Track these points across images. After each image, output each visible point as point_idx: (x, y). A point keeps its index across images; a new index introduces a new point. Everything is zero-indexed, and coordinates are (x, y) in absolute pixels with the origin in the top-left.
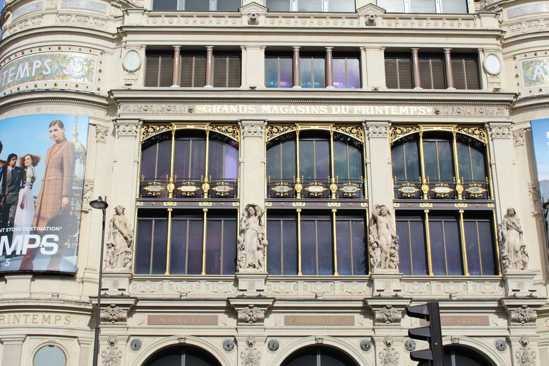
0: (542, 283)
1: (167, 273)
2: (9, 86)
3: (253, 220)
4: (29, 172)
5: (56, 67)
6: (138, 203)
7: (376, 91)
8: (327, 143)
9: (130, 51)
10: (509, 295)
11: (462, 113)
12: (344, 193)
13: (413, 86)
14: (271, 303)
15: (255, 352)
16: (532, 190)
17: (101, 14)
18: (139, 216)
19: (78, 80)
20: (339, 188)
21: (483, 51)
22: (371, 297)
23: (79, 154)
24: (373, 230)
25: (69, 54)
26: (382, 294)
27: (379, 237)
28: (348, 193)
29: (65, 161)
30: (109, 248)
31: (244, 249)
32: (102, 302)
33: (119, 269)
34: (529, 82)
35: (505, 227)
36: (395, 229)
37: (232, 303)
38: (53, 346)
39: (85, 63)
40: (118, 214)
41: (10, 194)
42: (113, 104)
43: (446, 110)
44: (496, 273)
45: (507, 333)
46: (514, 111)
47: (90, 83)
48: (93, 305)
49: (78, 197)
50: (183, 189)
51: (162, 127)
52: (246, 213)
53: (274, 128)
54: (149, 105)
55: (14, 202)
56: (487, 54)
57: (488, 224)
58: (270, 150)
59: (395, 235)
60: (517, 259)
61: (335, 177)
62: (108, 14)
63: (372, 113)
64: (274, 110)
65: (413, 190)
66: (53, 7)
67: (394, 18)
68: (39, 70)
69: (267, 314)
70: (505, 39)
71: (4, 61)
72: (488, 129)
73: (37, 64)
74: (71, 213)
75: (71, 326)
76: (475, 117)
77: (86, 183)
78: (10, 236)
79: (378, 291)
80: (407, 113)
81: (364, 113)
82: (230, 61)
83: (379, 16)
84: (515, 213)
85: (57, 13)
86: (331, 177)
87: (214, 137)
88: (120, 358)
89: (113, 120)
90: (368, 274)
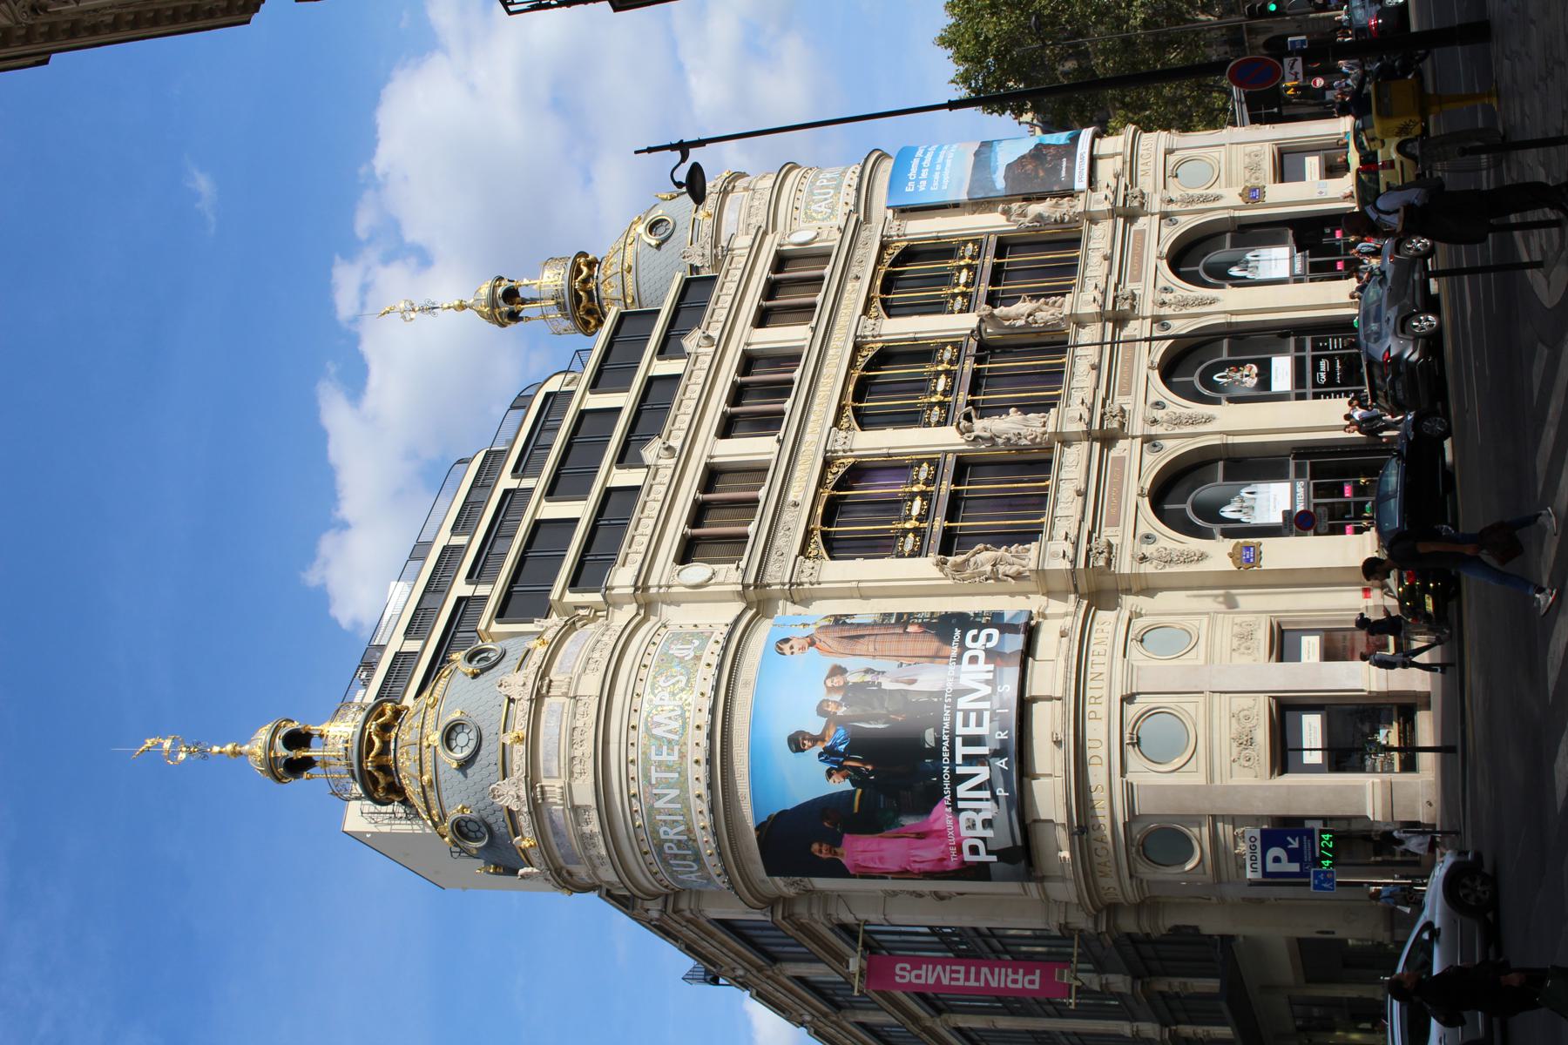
41: (886, 705)
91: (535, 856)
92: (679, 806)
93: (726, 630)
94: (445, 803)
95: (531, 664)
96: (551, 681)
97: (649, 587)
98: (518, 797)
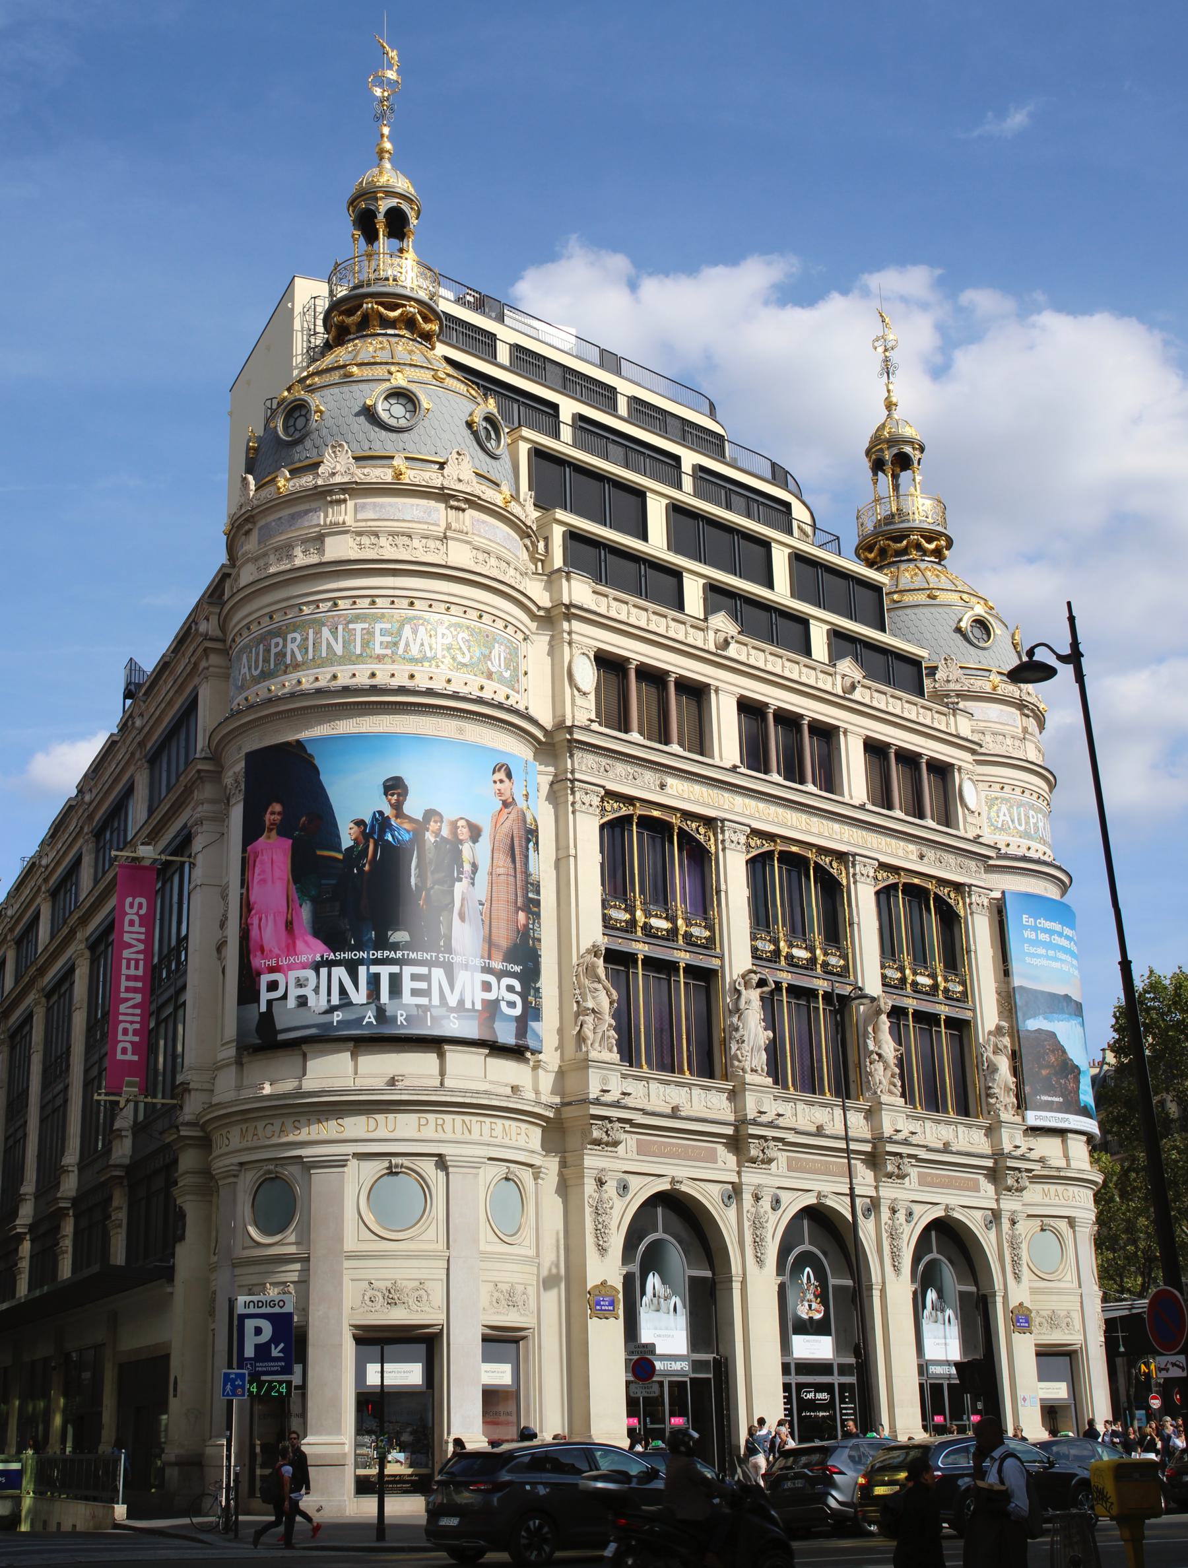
41: (436, 887)
91: (267, 493)
92: (324, 655)
93: (521, 707)
94: (326, 392)
95: (483, 488)
96: (463, 510)
97: (569, 621)
98: (334, 474)
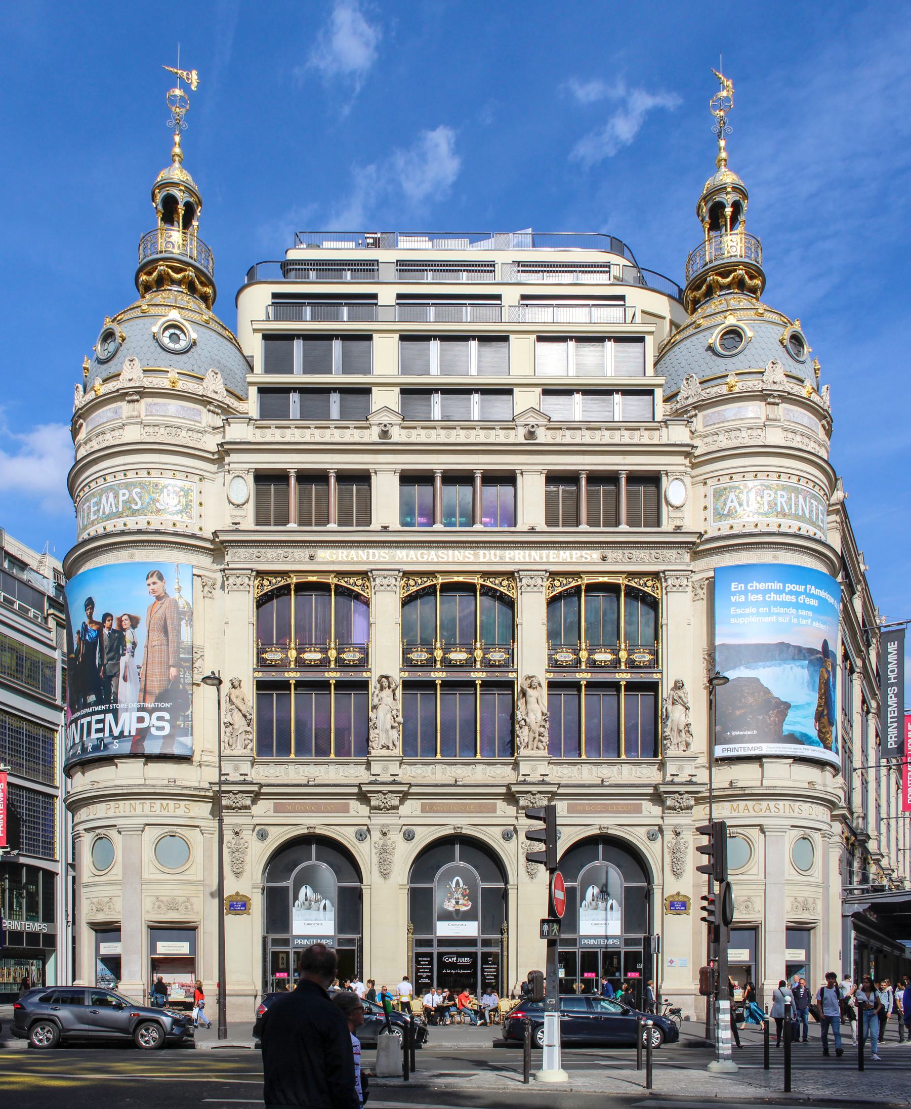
0: (705, 767)
1: (292, 756)
2: (92, 523)
3: (387, 693)
4: (128, 635)
5: (147, 499)
6: (256, 674)
7: (532, 531)
8: (473, 598)
9: (235, 477)
10: (667, 780)
11: (634, 558)
12: (490, 660)
13: (578, 524)
14: (406, 789)
15: (389, 842)
16: (706, 657)
17: (196, 424)
18: (258, 689)
19: (175, 516)
20: (484, 654)
21: (667, 474)
22: (515, 782)
23: (184, 613)
24: (522, 704)
25: (162, 482)
26: (528, 779)
27: (527, 714)
28: (495, 661)
29: (169, 622)
30: (226, 727)
31: (376, 728)
32: (223, 789)
33: (239, 751)
34: (719, 516)
35: (670, 701)
36: (546, 704)
37: (364, 789)
38: (174, 836)
39: (182, 493)
40: (234, 687)
42: (219, 549)
43: (614, 556)
44: (656, 755)
45: (660, 822)
46: (697, 555)
47: (190, 521)
48: (214, 791)
49: (186, 667)
50: (306, 656)
51: (279, 579)
52: (378, 686)
53: (411, 580)
54: (262, 550)
55: (115, 674)
56: (671, 478)
57: (653, 697)
58: (406, 607)
59: (545, 711)
60: (680, 740)
61: (481, 641)
62: (204, 425)
63: (527, 560)
64: (410, 556)
65: (569, 657)
66: (135, 414)
67: (561, 429)
68: (126, 502)
69: (402, 801)
70: (695, 457)
71: (82, 489)
72: (663, 580)
73: (124, 495)
74: (181, 686)
75: (192, 814)
76: (650, 564)
77: (195, 650)
78: (115, 713)
79: (523, 775)
80: (569, 560)
81: (517, 560)
82: (358, 490)
83: (542, 425)
84: (683, 685)
85: (142, 423)
86: (476, 641)
87: (343, 592)
88: (246, 848)
89: (221, 571)
90: (513, 756)
